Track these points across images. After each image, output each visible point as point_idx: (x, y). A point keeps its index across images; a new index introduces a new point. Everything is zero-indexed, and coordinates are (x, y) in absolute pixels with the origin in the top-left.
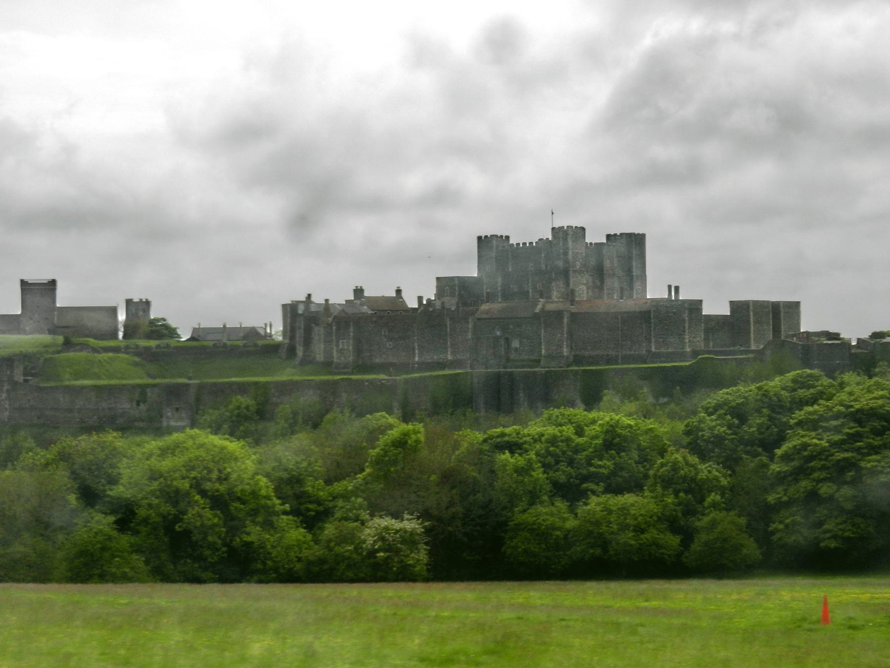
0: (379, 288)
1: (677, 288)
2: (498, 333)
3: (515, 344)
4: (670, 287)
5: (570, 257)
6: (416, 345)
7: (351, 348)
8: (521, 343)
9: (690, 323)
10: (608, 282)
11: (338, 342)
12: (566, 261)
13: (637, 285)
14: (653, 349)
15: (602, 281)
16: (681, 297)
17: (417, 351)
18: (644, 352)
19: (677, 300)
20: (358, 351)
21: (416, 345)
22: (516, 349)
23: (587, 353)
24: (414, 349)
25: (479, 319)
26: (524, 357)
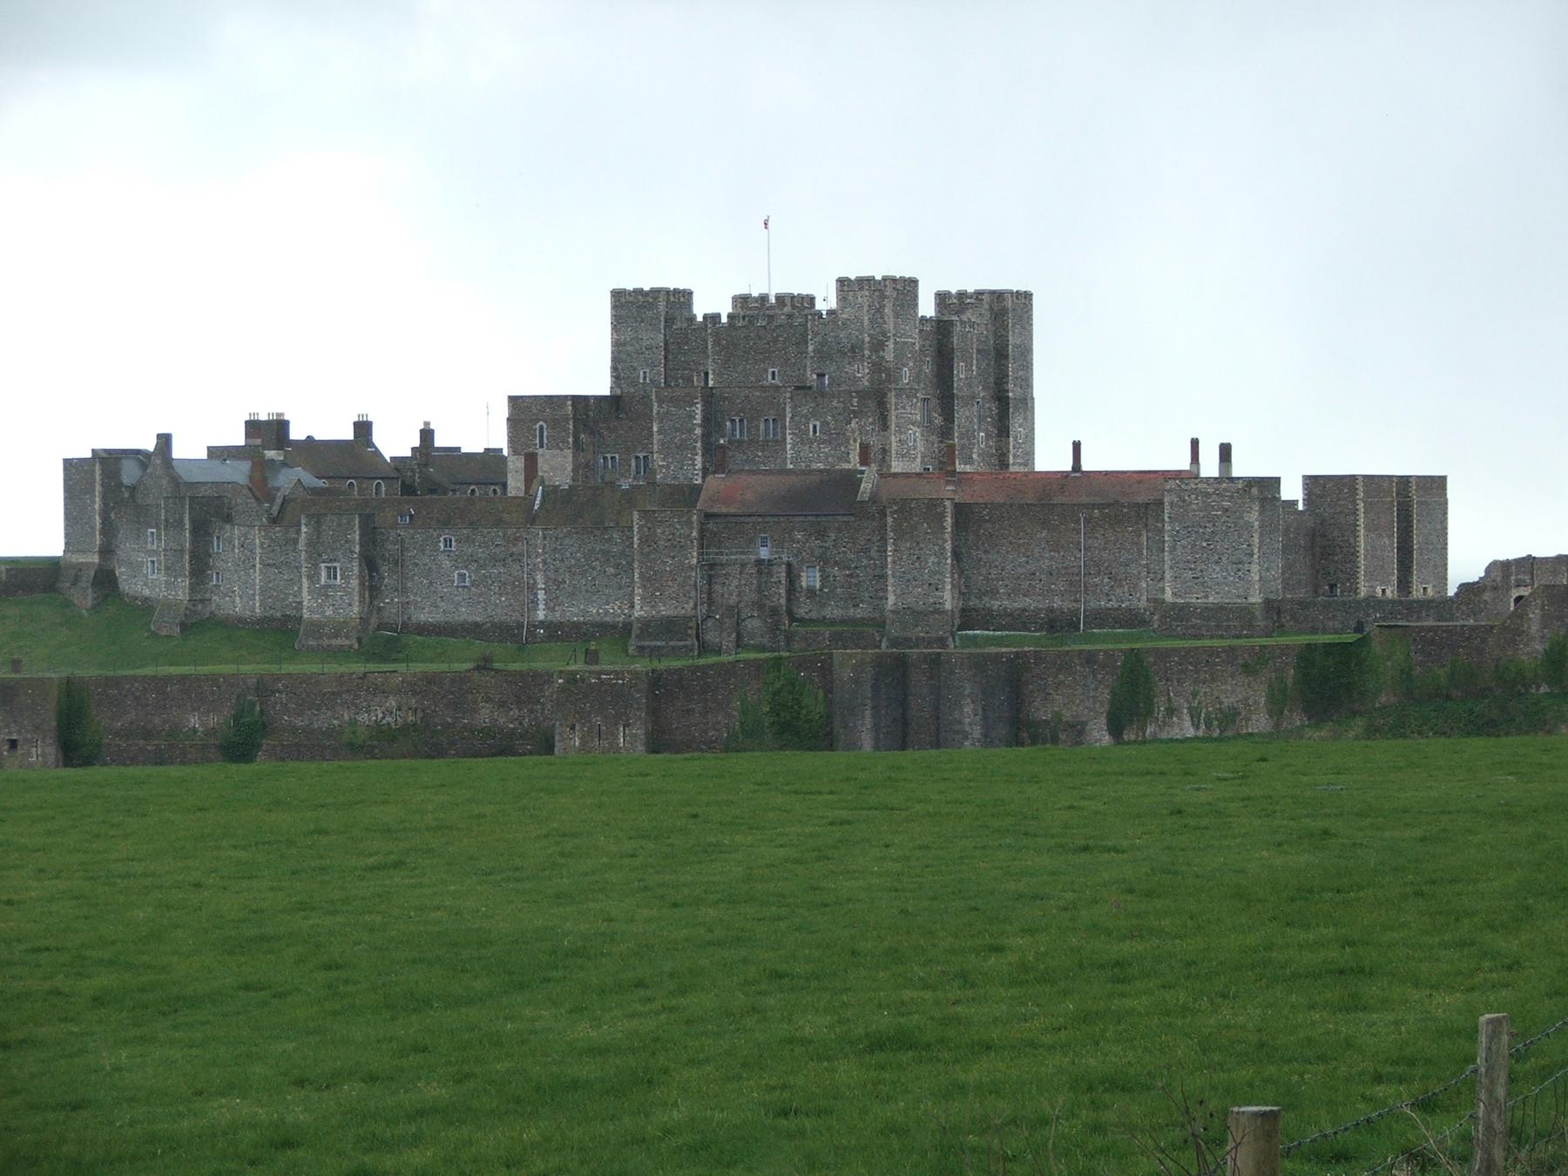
0: (320, 420)
1: (1225, 452)
2: (764, 553)
3: (810, 578)
4: (1195, 444)
5: (889, 354)
6: (539, 578)
7: (355, 583)
8: (824, 578)
9: (1261, 535)
10: (962, 414)
11: (316, 566)
12: (878, 367)
13: (1016, 427)
14: (1168, 596)
15: (948, 416)
16: (1240, 469)
17: (541, 595)
18: (1143, 603)
19: (1226, 478)
20: (372, 589)
21: (539, 578)
22: (811, 592)
23: (996, 604)
24: (532, 588)
25: (708, 516)
26: (833, 611)
